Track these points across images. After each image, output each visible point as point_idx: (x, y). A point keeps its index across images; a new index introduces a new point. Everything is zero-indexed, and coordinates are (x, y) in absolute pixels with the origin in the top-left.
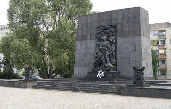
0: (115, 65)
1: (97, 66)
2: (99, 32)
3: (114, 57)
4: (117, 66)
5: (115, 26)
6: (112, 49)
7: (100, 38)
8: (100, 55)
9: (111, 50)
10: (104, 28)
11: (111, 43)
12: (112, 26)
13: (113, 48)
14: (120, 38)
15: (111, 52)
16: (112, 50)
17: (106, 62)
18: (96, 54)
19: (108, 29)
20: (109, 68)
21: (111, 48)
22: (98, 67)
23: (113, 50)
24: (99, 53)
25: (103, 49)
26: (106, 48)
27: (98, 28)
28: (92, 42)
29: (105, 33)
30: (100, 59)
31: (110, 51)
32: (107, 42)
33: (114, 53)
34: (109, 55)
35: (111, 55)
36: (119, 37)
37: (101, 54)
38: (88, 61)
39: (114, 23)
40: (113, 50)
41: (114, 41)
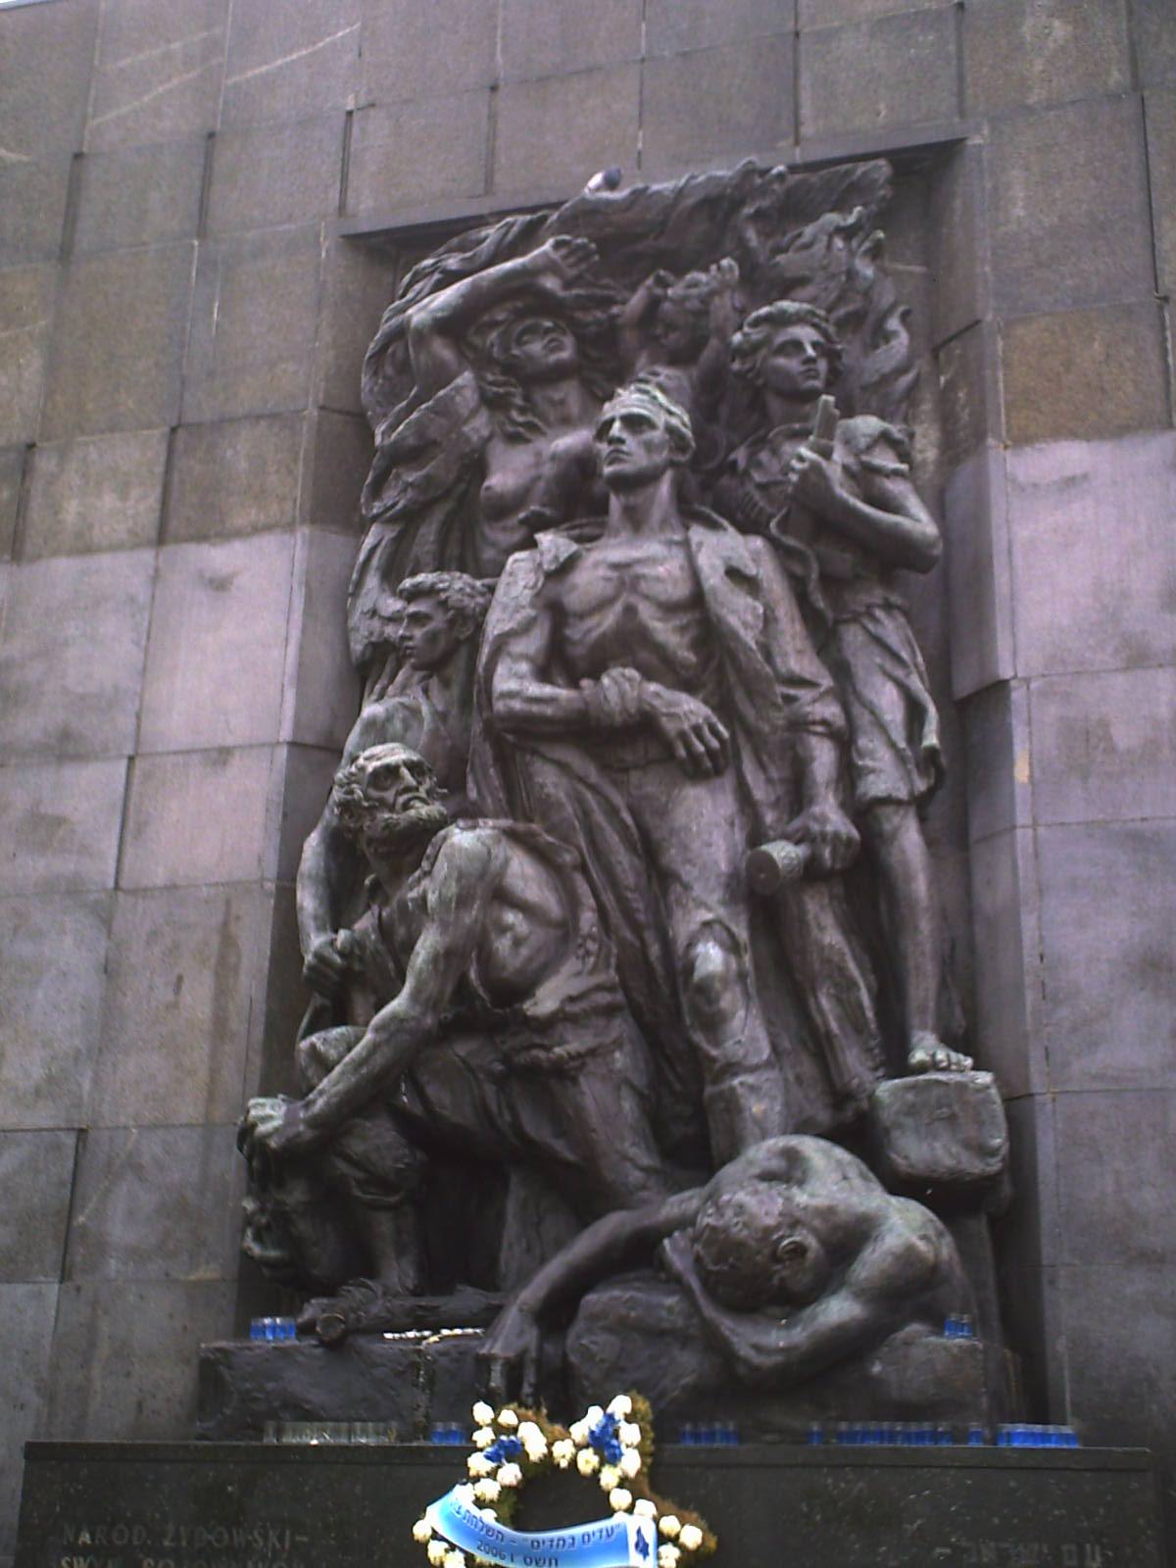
1: (363, 1264)
2: (452, 326)
3: (923, 987)
4: (1053, 1246)
6: (844, 741)
7: (477, 466)
8: (502, 896)
9: (823, 757)
13: (889, 702)
14: (1071, 455)
15: (830, 815)
16: (849, 773)
18: (308, 900)
20: (838, 1310)
21: (831, 711)
22: (399, 1272)
23: (884, 777)
26: (690, 709)
28: (220, 585)
31: (797, 794)
33: (909, 841)
35: (827, 932)
36: (1061, 431)
37: (523, 874)
38: (44, 1116)
40: (884, 777)
41: (920, 521)
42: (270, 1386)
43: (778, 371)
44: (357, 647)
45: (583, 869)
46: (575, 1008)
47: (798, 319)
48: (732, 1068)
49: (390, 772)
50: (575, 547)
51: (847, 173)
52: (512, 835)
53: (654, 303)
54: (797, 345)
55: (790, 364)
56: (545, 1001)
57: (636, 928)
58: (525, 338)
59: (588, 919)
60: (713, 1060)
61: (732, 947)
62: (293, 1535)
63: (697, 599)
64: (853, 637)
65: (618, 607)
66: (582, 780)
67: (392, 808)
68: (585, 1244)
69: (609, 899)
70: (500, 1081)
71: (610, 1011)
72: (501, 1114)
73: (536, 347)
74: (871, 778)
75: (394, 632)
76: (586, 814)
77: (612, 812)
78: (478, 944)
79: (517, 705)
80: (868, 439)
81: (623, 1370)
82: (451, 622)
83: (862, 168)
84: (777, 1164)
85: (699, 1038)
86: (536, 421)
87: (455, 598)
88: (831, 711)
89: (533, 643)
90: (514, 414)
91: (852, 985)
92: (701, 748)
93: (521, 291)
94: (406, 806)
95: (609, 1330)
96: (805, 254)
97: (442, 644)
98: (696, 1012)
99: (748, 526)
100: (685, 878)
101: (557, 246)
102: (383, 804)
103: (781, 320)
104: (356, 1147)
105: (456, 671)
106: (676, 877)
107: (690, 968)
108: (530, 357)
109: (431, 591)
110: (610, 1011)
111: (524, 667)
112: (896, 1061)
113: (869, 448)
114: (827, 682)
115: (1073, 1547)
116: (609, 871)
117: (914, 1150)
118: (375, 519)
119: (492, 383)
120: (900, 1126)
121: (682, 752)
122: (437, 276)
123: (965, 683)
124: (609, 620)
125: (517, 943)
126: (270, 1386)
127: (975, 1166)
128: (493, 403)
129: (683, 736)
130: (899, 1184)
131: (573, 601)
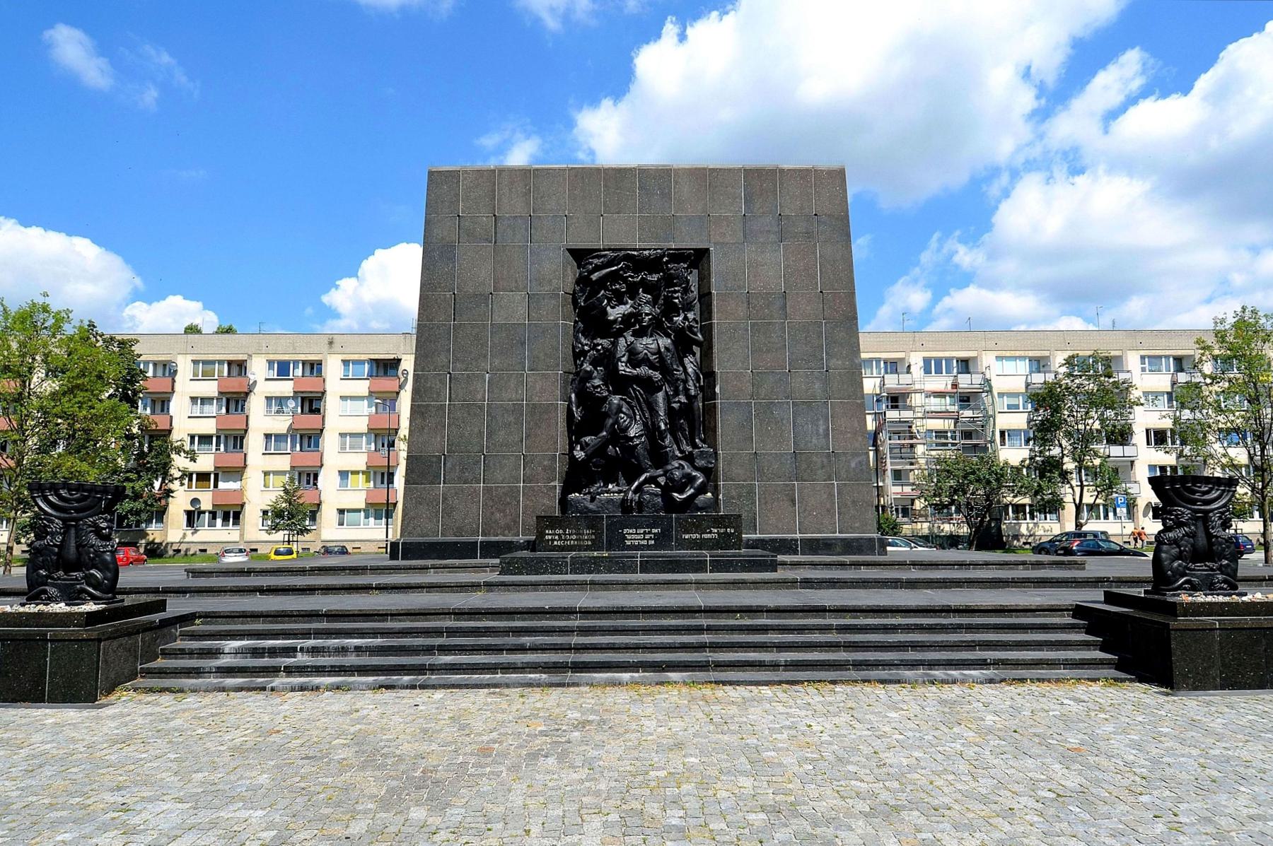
0: (709, 473)
2: (602, 280)
5: (699, 258)
6: (685, 382)
7: (606, 313)
11: (683, 343)
12: (678, 256)
15: (683, 399)
16: (686, 391)
17: (660, 458)
19: (653, 264)
21: (683, 376)
24: (615, 400)
25: (637, 379)
26: (657, 375)
27: (579, 255)
29: (632, 292)
30: (619, 436)
32: (664, 342)
34: (670, 411)
39: (687, 241)
47: (678, 291)
48: (666, 447)
49: (599, 386)
50: (633, 339)
52: (621, 399)
54: (677, 298)
55: (677, 301)
56: (632, 433)
57: (646, 418)
59: (638, 417)
61: (666, 424)
63: (659, 352)
64: (686, 361)
68: (642, 478)
71: (642, 436)
75: (586, 348)
78: (617, 422)
82: (604, 352)
84: (677, 465)
87: (605, 346)
88: (683, 376)
89: (624, 359)
91: (685, 430)
93: (614, 277)
99: (668, 336)
103: (676, 292)
106: (655, 410)
107: (660, 427)
109: (601, 344)
111: (623, 364)
112: (695, 446)
114: (681, 369)
117: (700, 463)
123: (705, 370)
124: (641, 356)
125: (625, 421)
127: (710, 466)
128: (609, 300)
130: (697, 469)
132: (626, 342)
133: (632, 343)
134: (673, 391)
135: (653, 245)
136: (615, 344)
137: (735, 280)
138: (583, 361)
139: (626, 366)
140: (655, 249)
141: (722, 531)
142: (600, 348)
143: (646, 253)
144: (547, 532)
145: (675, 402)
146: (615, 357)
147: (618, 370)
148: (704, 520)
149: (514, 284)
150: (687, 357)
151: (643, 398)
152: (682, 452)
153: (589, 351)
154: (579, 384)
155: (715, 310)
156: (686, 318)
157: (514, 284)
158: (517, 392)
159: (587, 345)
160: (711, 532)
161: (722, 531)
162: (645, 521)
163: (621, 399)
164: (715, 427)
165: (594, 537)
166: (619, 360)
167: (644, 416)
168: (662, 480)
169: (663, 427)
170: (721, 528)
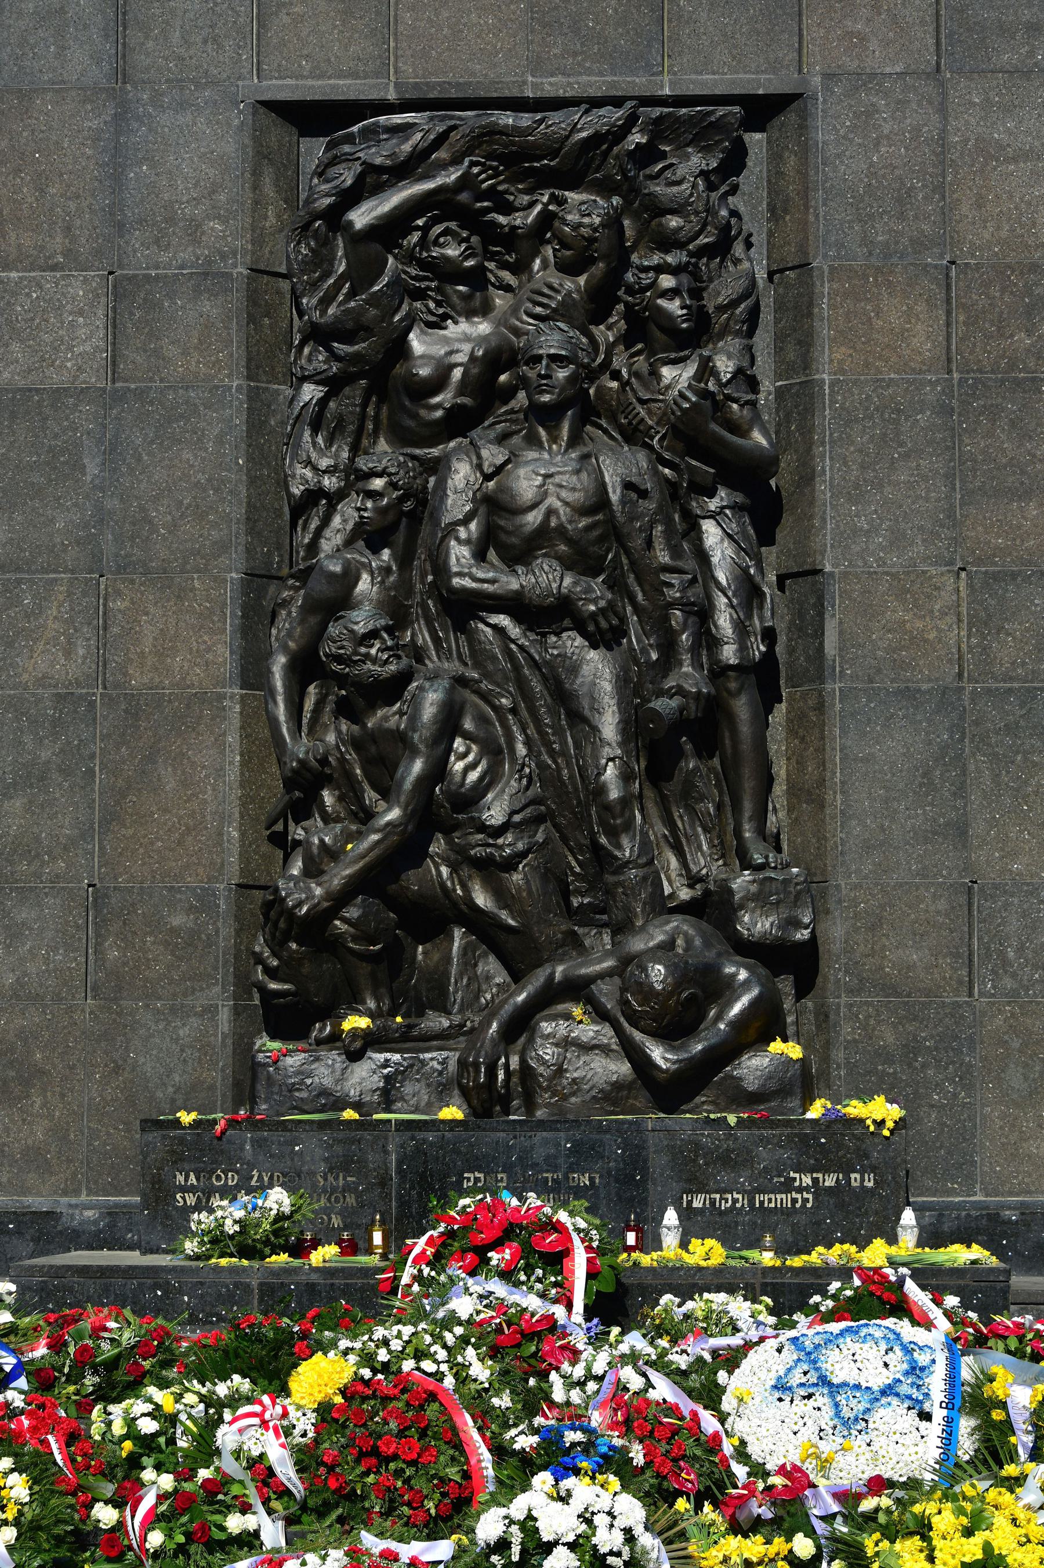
6: (704, 614)
7: (400, 349)
10: (494, 131)
42: (309, 1081)
43: (660, 309)
44: (296, 490)
45: (514, 711)
46: (517, 818)
51: (709, 114)
53: (547, 219)
55: (674, 307)
56: (495, 814)
57: (552, 753)
58: (442, 240)
59: (521, 750)
60: (616, 858)
61: (626, 777)
62: (344, 1179)
65: (543, 508)
66: (513, 641)
67: (374, 660)
69: (531, 731)
70: (454, 868)
72: (455, 890)
73: (452, 252)
74: (726, 647)
75: (329, 483)
76: (517, 668)
77: (535, 664)
79: (467, 583)
80: (729, 376)
81: (566, 1070)
82: (401, 500)
83: (721, 111)
85: (603, 840)
86: (449, 310)
90: (432, 305)
92: (604, 624)
94: (386, 662)
95: (557, 1045)
96: (675, 189)
97: (391, 517)
98: (602, 823)
100: (595, 722)
101: (473, 164)
102: (367, 656)
104: (353, 912)
105: (400, 537)
106: (586, 721)
107: (601, 790)
108: (446, 259)
110: (538, 820)
113: (729, 381)
114: (690, 564)
115: (858, 1176)
116: (533, 711)
118: (304, 379)
119: (415, 278)
120: (742, 907)
121: (591, 628)
122: (358, 168)
124: (533, 518)
126: (309, 1081)
129: (593, 615)
131: (504, 498)
132: (479, 467)
133: (499, 469)
134: (659, 647)
135: (595, 84)
136: (438, 467)
137: (902, 216)
138: (318, 533)
139: (480, 556)
140: (595, 103)
141: (830, 1181)
142: (378, 483)
143: (557, 121)
144: (180, 1178)
145: (660, 693)
146: (435, 521)
147: (441, 568)
148: (764, 1141)
149: (59, 241)
150: (713, 515)
151: (544, 679)
152: (693, 880)
153: (341, 495)
154: (302, 622)
155: (824, 332)
156: (706, 370)
157: (59, 241)
158: (68, 653)
159: (329, 471)
160: (788, 1186)
161: (830, 1181)
162: (545, 1142)
163: (460, 681)
164: (822, 782)
165: (351, 1200)
166: (451, 530)
167: (548, 744)
168: (606, 993)
169: (614, 794)
170: (826, 1171)
